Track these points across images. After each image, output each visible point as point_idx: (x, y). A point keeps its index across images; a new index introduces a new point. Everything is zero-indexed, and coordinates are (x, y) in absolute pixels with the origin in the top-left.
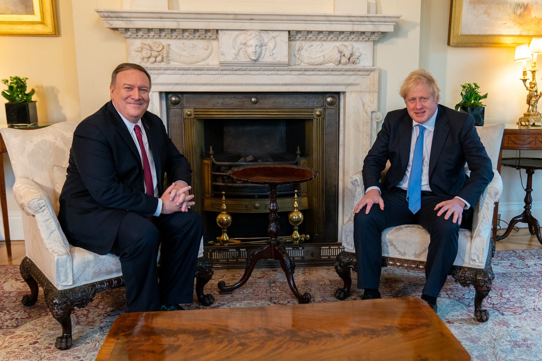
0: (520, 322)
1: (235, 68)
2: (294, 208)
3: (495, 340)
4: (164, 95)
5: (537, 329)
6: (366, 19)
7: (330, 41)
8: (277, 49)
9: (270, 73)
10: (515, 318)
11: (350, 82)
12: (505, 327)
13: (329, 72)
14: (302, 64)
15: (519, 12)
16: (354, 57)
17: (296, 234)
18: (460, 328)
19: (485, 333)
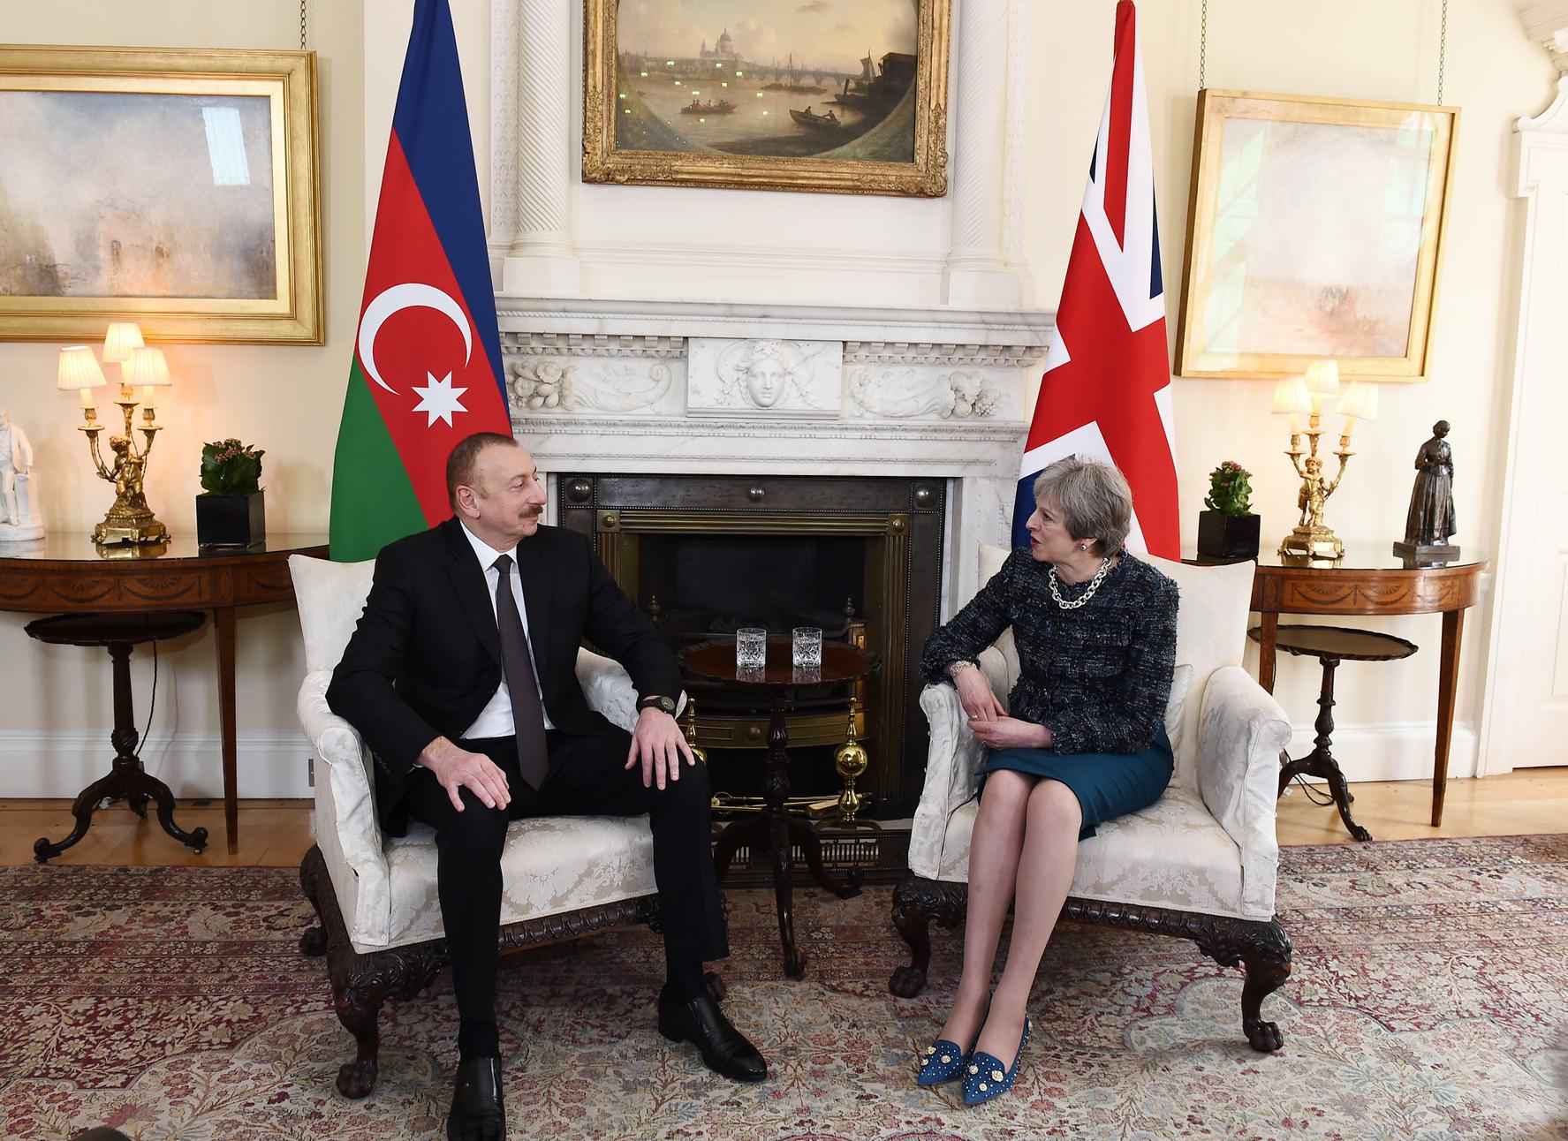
0: (1442, 1053)
1: (722, 422)
2: (849, 737)
3: (1402, 1107)
4: (553, 480)
5: (1490, 1073)
6: (1018, 319)
7: (932, 364)
8: (818, 382)
9: (797, 433)
10: (1425, 1041)
11: (972, 456)
12: (1410, 1067)
13: (929, 435)
14: (868, 415)
15: (1329, 306)
16: (984, 401)
17: (854, 798)
18: (1305, 1070)
19: (1370, 1084)
